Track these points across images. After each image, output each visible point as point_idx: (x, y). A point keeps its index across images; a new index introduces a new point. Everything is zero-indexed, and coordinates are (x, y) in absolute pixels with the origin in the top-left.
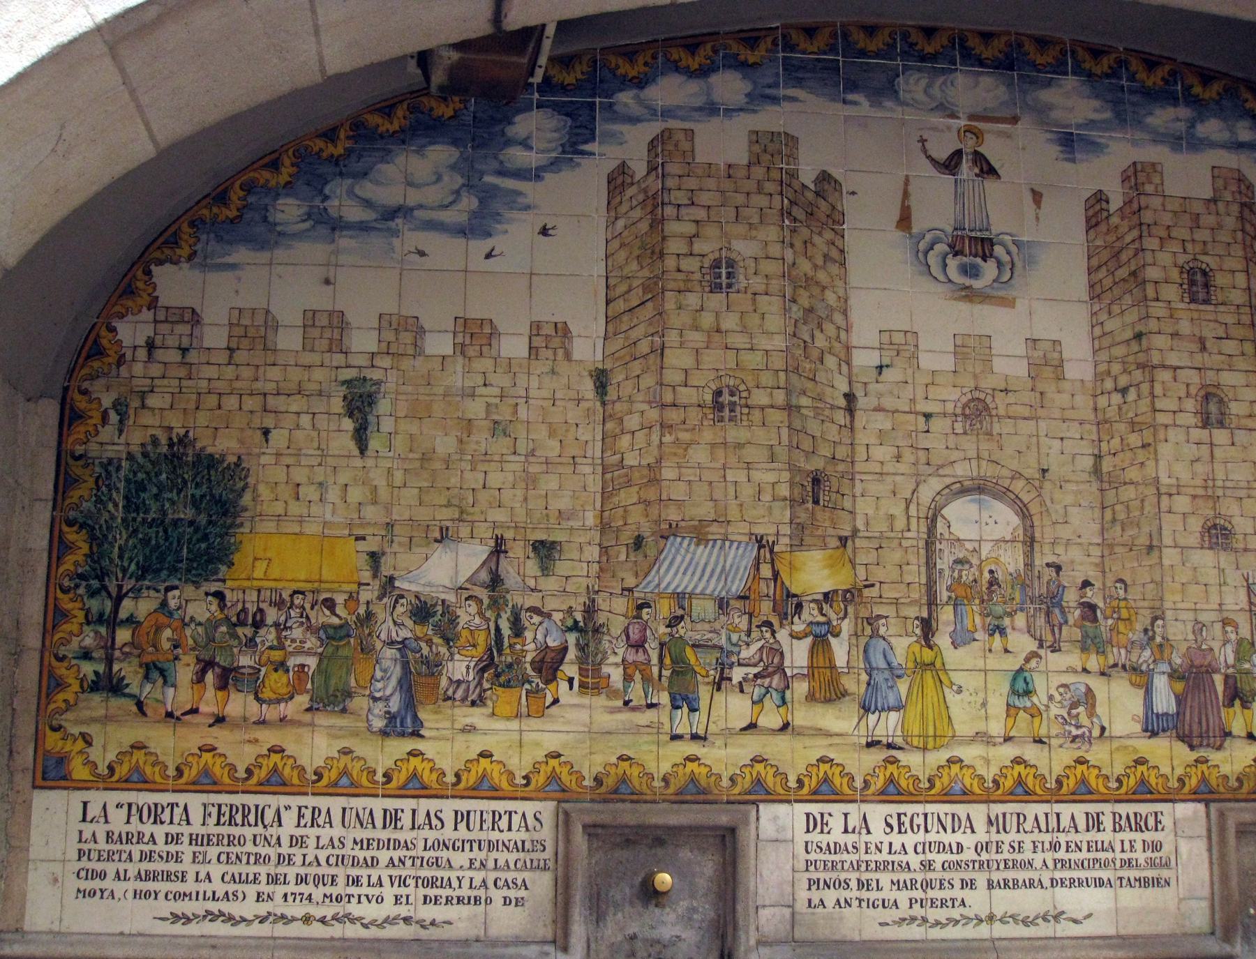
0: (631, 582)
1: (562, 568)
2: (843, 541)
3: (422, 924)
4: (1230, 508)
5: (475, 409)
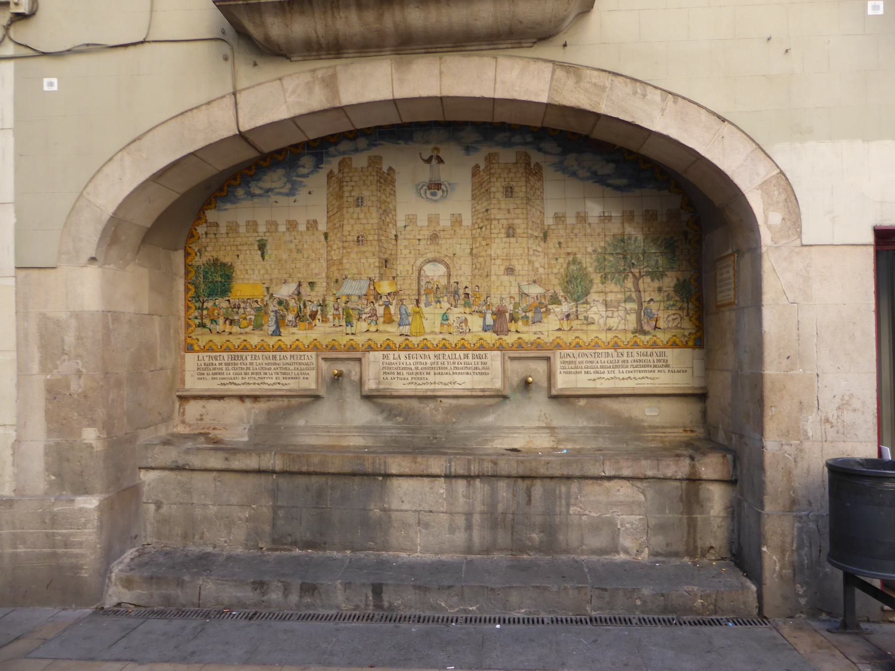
1: (316, 289)
2: (394, 278)
4: (515, 262)
5: (292, 246)
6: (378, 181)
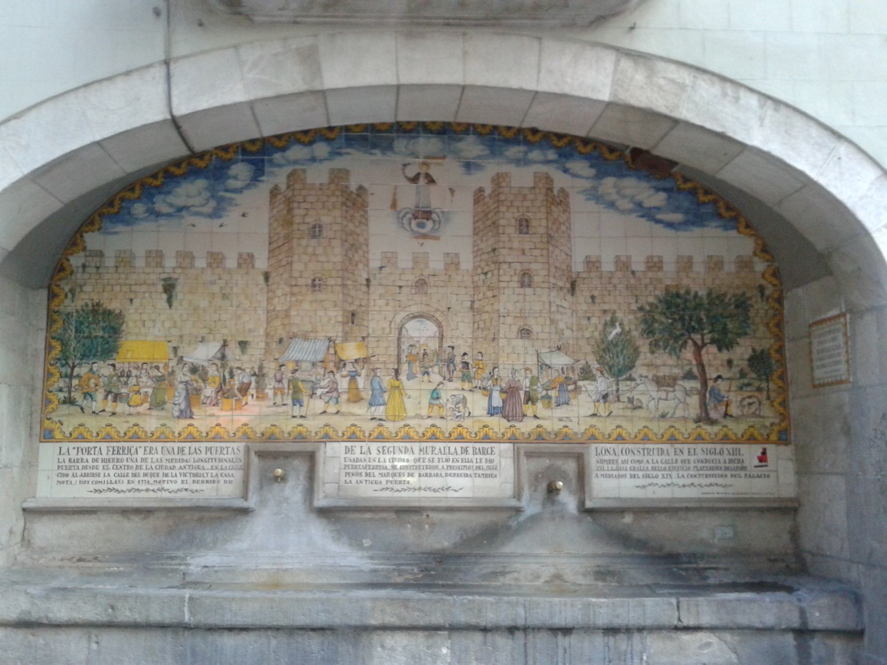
0: (277, 356)
1: (250, 351)
2: (364, 338)
3: (192, 491)
5: (215, 289)
6: (344, 204)
